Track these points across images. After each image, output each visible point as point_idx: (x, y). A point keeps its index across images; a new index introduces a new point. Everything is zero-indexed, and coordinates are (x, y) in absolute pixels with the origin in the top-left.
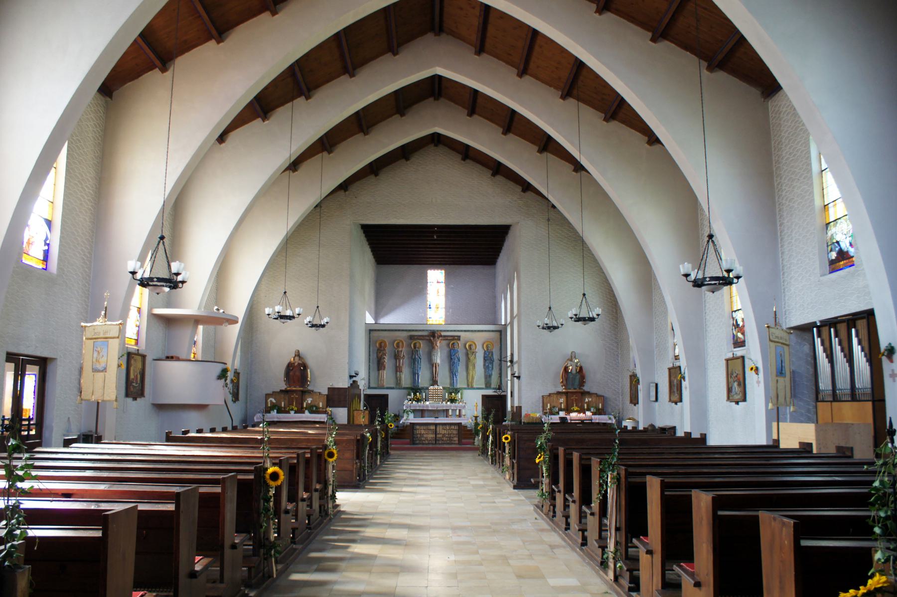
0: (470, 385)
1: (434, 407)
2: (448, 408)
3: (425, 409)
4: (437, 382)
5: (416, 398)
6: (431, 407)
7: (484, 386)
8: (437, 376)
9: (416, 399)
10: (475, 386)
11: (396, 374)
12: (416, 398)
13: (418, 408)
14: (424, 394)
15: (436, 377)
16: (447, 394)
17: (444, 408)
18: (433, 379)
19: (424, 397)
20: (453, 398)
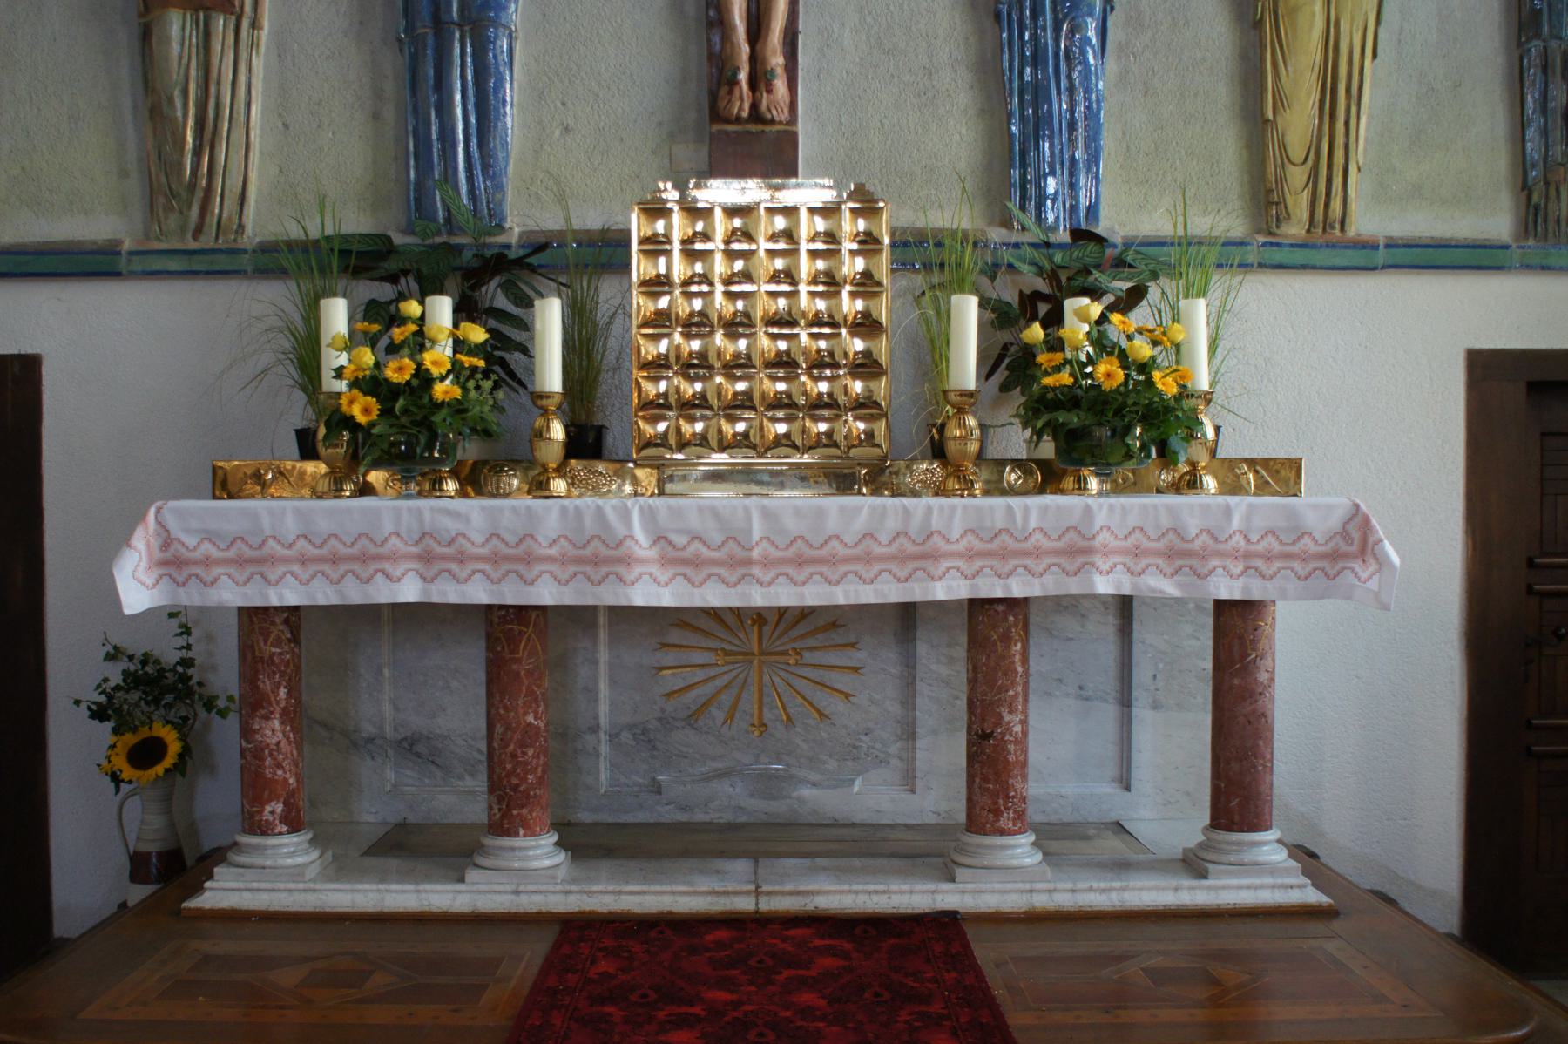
0: (1299, 205)
1: (740, 564)
2: (1017, 590)
3: (546, 593)
4: (792, 139)
5: (372, 384)
6: (678, 560)
7: (1498, 223)
8: (777, 60)
9: (361, 409)
10: (1367, 221)
11: (146, 36)
12: (372, 384)
13: (409, 591)
14: (550, 317)
15: (760, 79)
16: (968, 311)
17: (949, 587)
18: (716, 115)
19: (551, 376)
20: (1108, 373)
